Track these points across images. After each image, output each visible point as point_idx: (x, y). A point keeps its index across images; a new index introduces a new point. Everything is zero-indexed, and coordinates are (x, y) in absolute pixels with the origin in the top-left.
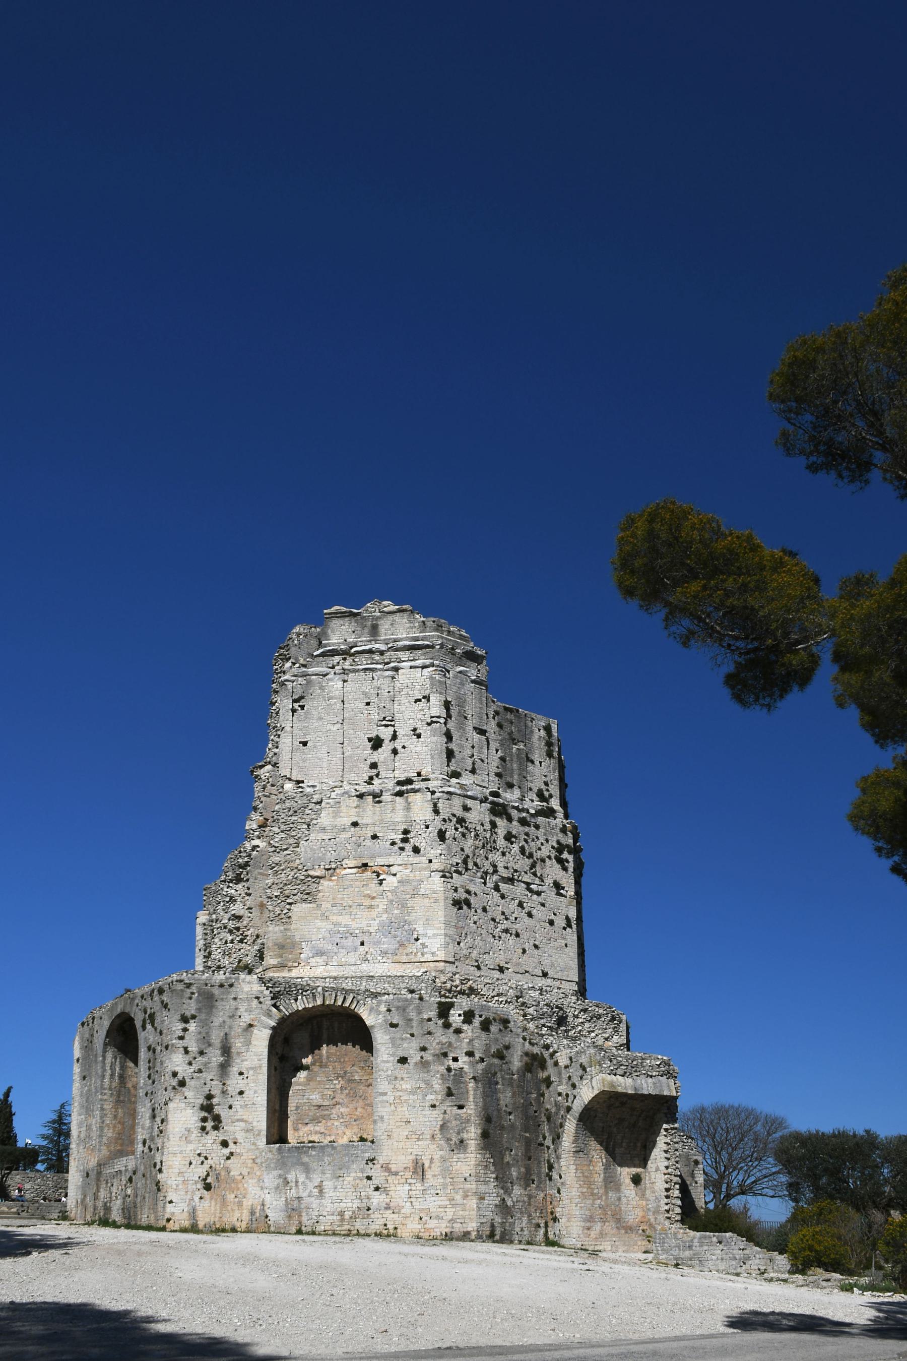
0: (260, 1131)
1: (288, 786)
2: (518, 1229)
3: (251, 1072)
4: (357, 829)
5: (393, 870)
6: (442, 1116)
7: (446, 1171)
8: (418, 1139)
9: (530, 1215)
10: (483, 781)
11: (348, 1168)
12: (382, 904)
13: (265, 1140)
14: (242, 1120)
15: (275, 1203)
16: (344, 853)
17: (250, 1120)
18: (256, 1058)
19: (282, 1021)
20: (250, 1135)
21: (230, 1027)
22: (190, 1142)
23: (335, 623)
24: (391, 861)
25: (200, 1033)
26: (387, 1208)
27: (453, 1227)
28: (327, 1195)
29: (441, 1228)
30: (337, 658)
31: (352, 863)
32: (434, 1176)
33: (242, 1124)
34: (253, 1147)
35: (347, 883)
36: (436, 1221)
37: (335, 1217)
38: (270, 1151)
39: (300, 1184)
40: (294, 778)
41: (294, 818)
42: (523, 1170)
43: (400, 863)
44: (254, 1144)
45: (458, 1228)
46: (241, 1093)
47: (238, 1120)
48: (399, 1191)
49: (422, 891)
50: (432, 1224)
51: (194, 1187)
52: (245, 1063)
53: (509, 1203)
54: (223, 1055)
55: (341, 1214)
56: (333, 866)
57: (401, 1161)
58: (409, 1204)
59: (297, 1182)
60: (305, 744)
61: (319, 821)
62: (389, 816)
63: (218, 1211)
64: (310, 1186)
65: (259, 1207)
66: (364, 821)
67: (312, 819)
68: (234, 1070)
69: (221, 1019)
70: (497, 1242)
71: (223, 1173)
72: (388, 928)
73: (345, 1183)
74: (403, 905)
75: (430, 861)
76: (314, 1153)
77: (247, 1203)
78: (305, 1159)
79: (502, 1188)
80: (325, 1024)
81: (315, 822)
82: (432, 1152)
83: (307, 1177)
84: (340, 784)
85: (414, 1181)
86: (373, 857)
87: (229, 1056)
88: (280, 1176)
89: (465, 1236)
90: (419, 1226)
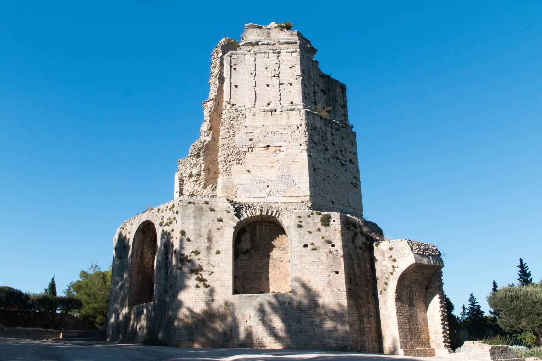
1: (228, 106)
4: (264, 128)
5: (282, 149)
6: (328, 278)
12: (277, 166)
13: (231, 292)
17: (223, 280)
19: (239, 224)
21: (212, 227)
23: (250, 31)
26: (301, 332)
27: (337, 343)
30: (251, 47)
33: (219, 283)
41: (232, 122)
42: (367, 308)
44: (226, 294)
47: (217, 280)
52: (220, 247)
54: (208, 243)
58: (312, 329)
59: (250, 317)
60: (236, 86)
66: (268, 124)
68: (214, 251)
69: (207, 222)
75: (301, 145)
80: (258, 227)
86: (272, 142)
87: (211, 243)
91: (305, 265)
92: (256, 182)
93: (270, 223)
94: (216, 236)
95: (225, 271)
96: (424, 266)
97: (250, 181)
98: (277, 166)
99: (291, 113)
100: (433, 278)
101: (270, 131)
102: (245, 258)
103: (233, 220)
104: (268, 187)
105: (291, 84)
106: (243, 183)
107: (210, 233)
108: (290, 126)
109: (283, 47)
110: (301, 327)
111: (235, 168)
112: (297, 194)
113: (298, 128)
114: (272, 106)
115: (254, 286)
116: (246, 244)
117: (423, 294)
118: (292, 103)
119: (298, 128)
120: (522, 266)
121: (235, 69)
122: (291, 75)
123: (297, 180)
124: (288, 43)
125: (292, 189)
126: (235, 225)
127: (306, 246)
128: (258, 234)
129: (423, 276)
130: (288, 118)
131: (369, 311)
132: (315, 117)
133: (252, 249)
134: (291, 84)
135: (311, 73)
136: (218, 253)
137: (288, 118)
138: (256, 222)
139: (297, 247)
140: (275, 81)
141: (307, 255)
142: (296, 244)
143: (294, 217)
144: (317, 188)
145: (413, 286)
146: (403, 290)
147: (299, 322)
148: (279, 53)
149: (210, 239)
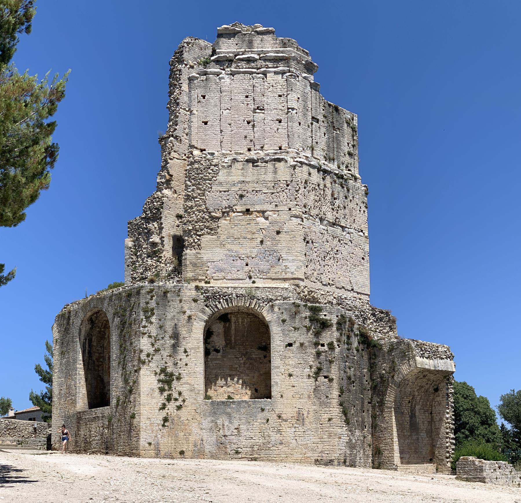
0: (199, 391)
2: (358, 458)
3: (193, 351)
5: (266, 214)
7: (318, 419)
8: (300, 398)
9: (364, 449)
10: (317, 155)
11: (256, 417)
14: (188, 383)
15: (209, 439)
16: (234, 202)
18: (195, 342)
19: (210, 317)
20: (193, 394)
22: (153, 398)
24: (265, 207)
25: (158, 323)
26: (281, 444)
27: (322, 457)
28: (243, 435)
29: (316, 456)
31: (239, 208)
32: (310, 422)
34: (195, 402)
35: (237, 222)
36: (312, 452)
37: (248, 449)
38: (206, 405)
39: (225, 427)
40: (199, 147)
41: (200, 175)
43: (271, 209)
45: (326, 457)
46: (186, 365)
47: (185, 383)
48: (289, 432)
49: (285, 229)
50: (309, 454)
51: (157, 428)
52: (189, 345)
53: (354, 441)
55: (252, 447)
56: (228, 210)
57: (289, 412)
58: (295, 441)
59: (223, 425)
60: (206, 123)
61: (217, 178)
62: (263, 176)
63: (173, 445)
64: (232, 428)
65: (199, 442)
66: (247, 180)
67: (213, 177)
70: (348, 466)
71: (176, 419)
73: (254, 426)
74: (273, 239)
75: (290, 209)
76: (234, 406)
77: (192, 439)
78: (229, 410)
79: (350, 431)
80: (233, 319)
81: (214, 179)
82: (308, 406)
83: (230, 422)
84: (229, 152)
85: (297, 426)
88: (212, 421)
89: (329, 463)
90: (301, 456)
91: (288, 367)
92: (232, 258)
93: (248, 314)
94: (183, 332)
95: (194, 373)
96: (429, 371)
99: (278, 164)
100: (442, 384)
101: (251, 190)
102: (219, 357)
103: (203, 312)
104: (247, 265)
105: (280, 122)
106: (215, 259)
108: (276, 182)
109: (270, 64)
110: (281, 438)
111: (206, 239)
112: (283, 276)
113: (288, 186)
114: (253, 155)
116: (219, 341)
117: (428, 403)
118: (280, 148)
122: (281, 107)
123: (284, 256)
124: (276, 60)
125: (277, 269)
126: (206, 318)
127: (290, 345)
128: (233, 328)
129: (429, 383)
130: (275, 172)
131: (363, 422)
132: (312, 170)
134: (280, 122)
135: (309, 103)
136: (185, 352)
137: (275, 172)
138: (231, 313)
139: (280, 346)
140: (259, 116)
141: (292, 355)
144: (309, 266)
145: (417, 393)
146: (403, 398)
147: (279, 431)
148: (265, 74)
149: (176, 336)
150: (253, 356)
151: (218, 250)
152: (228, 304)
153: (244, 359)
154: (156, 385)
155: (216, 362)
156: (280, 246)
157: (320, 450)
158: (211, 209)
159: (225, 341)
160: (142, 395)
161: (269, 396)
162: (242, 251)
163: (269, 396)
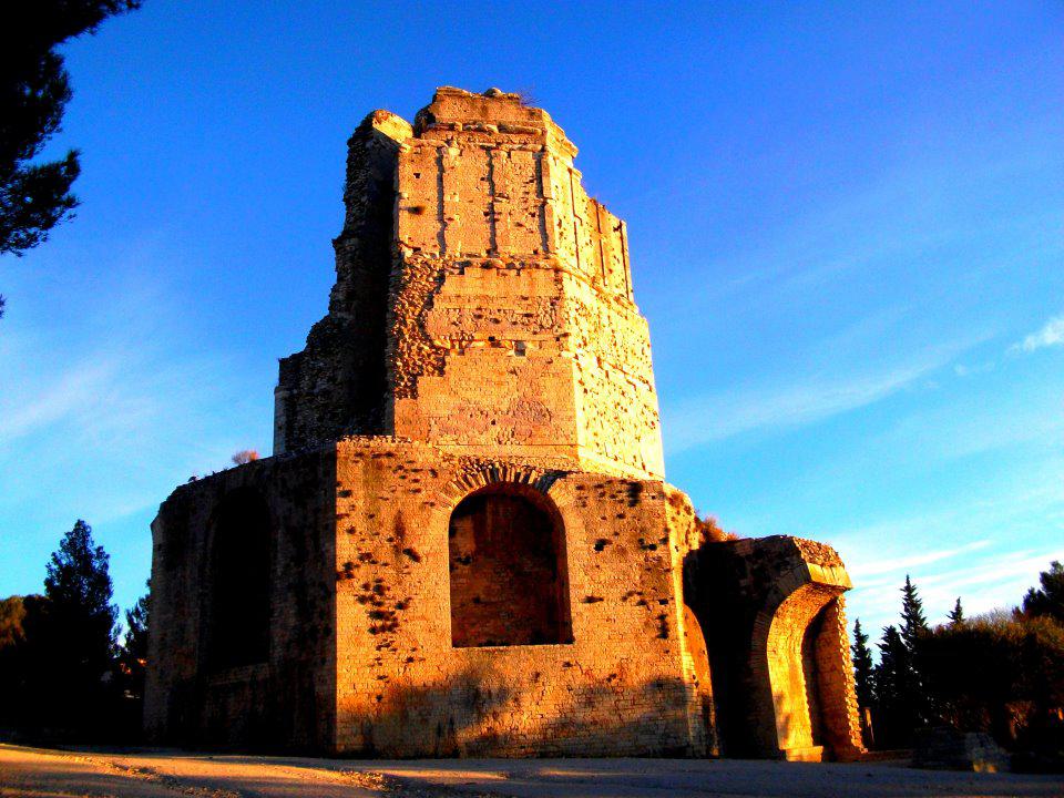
3: (431, 559)
13: (450, 642)
22: (360, 644)
33: (422, 623)
36: (647, 737)
38: (457, 656)
66: (489, 293)
72: (519, 408)
76: (507, 658)
77: (434, 721)
94: (412, 524)
97: (456, 412)
98: (512, 380)
101: (495, 308)
104: (493, 423)
107: (400, 518)
115: (486, 629)
119: (552, 304)
120: (909, 589)
121: (418, 175)
128: (489, 521)
130: (532, 284)
133: (477, 552)
137: (532, 284)
142: (579, 544)
143: (572, 487)
150: (526, 569)
151: (443, 398)
152: (487, 480)
153: (510, 575)
154: (365, 622)
155: (461, 580)
156: (545, 396)
157: (662, 732)
158: (433, 335)
159: (477, 543)
160: (339, 640)
161: (570, 640)
162: (486, 403)
163: (570, 640)
